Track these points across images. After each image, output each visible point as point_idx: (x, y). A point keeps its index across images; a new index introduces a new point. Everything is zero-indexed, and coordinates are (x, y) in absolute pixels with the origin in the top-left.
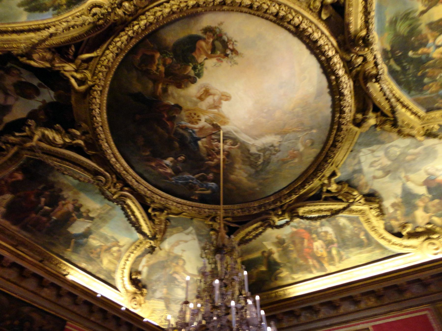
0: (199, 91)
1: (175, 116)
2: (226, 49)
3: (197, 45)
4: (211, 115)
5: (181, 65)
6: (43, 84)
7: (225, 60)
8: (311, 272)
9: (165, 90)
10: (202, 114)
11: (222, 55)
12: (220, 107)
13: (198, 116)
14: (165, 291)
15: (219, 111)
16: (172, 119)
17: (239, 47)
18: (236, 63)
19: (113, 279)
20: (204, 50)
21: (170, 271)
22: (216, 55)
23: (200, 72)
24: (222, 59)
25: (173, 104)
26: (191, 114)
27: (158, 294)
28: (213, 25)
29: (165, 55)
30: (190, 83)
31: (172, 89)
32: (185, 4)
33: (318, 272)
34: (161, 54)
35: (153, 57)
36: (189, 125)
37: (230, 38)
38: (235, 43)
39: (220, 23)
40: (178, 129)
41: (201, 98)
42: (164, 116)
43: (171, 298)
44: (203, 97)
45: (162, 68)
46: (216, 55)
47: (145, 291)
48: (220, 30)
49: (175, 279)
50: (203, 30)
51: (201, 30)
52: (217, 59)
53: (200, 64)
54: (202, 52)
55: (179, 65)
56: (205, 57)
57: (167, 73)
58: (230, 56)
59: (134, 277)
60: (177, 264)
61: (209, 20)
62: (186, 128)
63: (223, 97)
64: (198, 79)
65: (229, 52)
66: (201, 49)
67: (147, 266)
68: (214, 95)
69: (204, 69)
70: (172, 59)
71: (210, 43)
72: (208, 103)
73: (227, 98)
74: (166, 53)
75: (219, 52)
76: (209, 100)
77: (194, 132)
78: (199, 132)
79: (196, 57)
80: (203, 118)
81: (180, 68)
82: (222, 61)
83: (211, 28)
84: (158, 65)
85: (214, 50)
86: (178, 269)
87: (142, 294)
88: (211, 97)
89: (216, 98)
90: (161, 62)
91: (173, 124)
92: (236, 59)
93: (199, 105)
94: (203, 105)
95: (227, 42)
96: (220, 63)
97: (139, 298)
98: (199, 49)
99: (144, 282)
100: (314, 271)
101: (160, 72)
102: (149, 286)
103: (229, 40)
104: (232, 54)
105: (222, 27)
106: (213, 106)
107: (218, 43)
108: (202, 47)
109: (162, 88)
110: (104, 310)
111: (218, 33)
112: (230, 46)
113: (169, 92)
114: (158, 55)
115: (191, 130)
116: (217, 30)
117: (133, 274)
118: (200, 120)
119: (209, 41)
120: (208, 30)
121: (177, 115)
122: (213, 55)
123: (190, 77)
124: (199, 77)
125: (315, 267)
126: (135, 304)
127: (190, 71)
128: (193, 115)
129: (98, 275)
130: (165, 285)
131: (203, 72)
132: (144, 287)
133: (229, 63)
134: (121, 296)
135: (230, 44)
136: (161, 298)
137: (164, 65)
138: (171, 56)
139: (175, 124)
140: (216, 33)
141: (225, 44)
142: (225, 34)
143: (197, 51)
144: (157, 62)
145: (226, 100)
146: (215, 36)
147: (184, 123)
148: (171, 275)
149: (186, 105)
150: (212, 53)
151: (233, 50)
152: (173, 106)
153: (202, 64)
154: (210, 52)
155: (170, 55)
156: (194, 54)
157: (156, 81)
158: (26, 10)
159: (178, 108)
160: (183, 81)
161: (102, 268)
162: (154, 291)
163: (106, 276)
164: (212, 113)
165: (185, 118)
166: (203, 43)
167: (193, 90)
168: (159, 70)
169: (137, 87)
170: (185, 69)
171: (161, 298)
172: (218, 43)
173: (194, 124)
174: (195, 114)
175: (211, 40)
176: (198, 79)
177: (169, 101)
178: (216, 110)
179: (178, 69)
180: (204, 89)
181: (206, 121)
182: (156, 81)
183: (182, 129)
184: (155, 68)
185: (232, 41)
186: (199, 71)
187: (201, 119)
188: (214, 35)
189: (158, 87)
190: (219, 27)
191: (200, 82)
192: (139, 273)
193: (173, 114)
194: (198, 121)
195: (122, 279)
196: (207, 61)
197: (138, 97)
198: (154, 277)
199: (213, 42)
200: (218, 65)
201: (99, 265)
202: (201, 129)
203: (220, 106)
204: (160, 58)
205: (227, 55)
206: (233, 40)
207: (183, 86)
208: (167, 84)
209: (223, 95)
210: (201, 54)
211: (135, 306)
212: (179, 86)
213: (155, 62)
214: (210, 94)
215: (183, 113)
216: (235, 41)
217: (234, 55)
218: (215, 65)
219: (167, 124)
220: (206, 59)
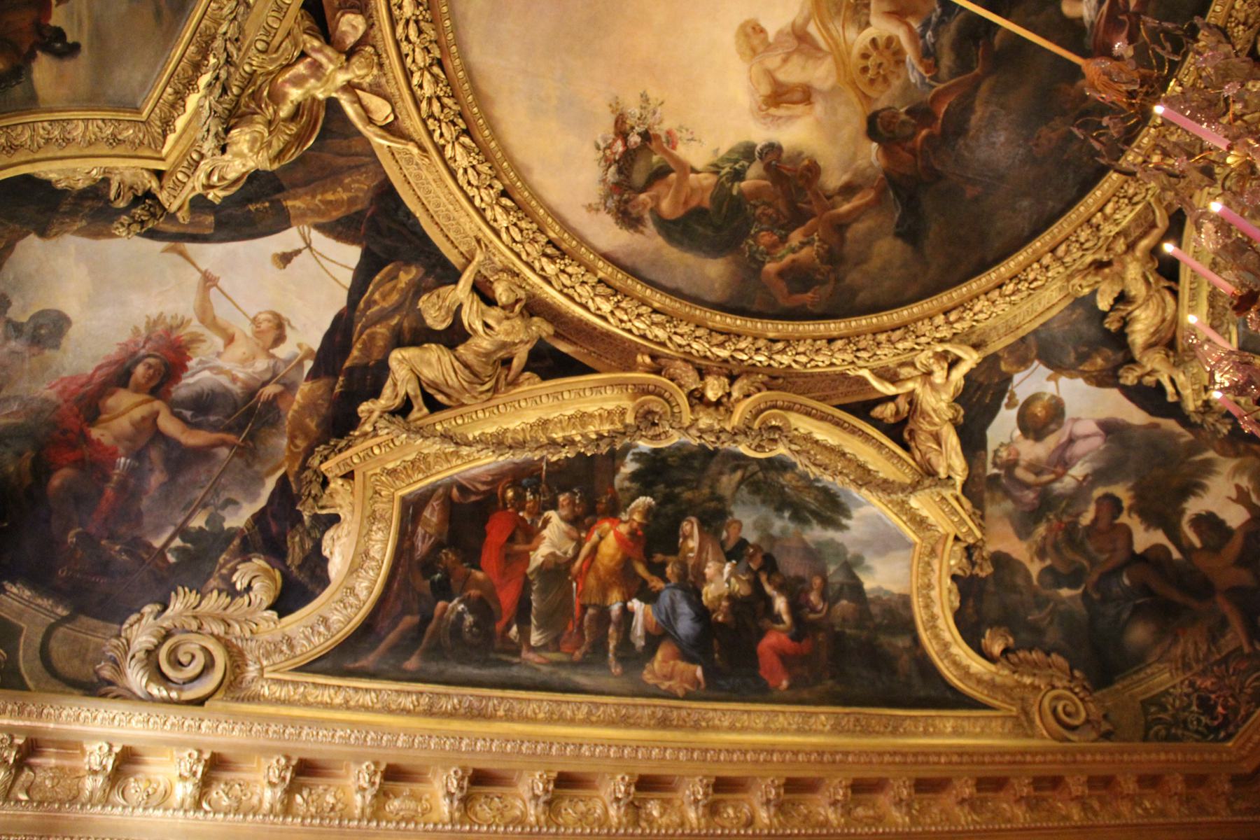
0: (790, 118)
1: (908, 112)
2: (634, 150)
3: (681, 212)
4: (836, 27)
5: (755, 207)
6: (1005, 400)
7: (660, 130)
9: (848, 190)
10: (849, 54)
11: (653, 146)
12: (793, 24)
13: (865, 56)
15: (807, 21)
16: (921, 113)
17: (605, 128)
18: (645, 98)
20: (678, 192)
22: (666, 158)
23: (736, 156)
24: (664, 139)
25: (875, 145)
26: (872, 81)
28: (609, 219)
29: (758, 257)
30: (784, 155)
31: (833, 179)
32: (617, 313)
34: (763, 263)
35: (781, 274)
36: (910, 56)
37: (603, 163)
38: (602, 145)
39: (593, 212)
40: (944, 71)
41: (806, 95)
42: (927, 138)
44: (797, 96)
45: (796, 237)
46: (666, 158)
48: (606, 198)
50: (637, 230)
51: (642, 232)
52: (674, 148)
53: (717, 173)
54: (686, 190)
55: (758, 211)
56: (692, 176)
57: (798, 217)
58: (637, 129)
61: (607, 234)
62: (928, 55)
63: (761, 49)
64: (758, 148)
65: (634, 139)
66: (682, 199)
68: (769, 73)
69: (723, 151)
70: (755, 237)
71: (652, 193)
72: (803, 68)
73: (752, 32)
74: (752, 258)
75: (655, 158)
76: (793, 73)
77: (926, 26)
78: (914, 13)
79: (708, 195)
80: (858, 40)
81: (764, 203)
82: (669, 133)
83: (617, 219)
84: (793, 251)
85: (660, 174)
88: (782, 76)
89: (773, 61)
90: (782, 251)
91: (937, 97)
92: (633, 110)
93: (827, 85)
94: (821, 74)
95: (616, 162)
96: (679, 134)
98: (686, 203)
101: (807, 234)
103: (608, 162)
104: (633, 128)
105: (595, 199)
106: (804, 46)
107: (639, 177)
108: (675, 203)
109: (848, 201)
111: (616, 197)
112: (619, 147)
113: (845, 178)
114: (771, 267)
115: (923, 37)
116: (611, 203)
118: (874, 41)
119: (649, 200)
120: (628, 218)
121: (902, 110)
122: (672, 166)
123: (768, 167)
124: (754, 146)
127: (754, 176)
128: (871, 74)
131: (731, 151)
133: (657, 115)
135: (615, 154)
137: (784, 240)
138: (751, 242)
139: (934, 90)
140: (619, 201)
141: (625, 163)
142: (604, 181)
143: (693, 203)
144: (790, 257)
145: (759, 30)
146: (626, 196)
147: (914, 70)
149: (852, 118)
150: (672, 171)
151: (622, 132)
152: (880, 143)
153: (715, 168)
154: (673, 176)
155: (750, 246)
156: (707, 203)
157: (840, 226)
158: (849, 517)
159: (875, 127)
160: (791, 178)
164: (828, 30)
165: (896, 83)
166: (665, 206)
167: (797, 133)
168: (805, 240)
169: (888, 248)
170: (757, 193)
172: (639, 177)
173: (899, 42)
174: (865, 70)
175: (643, 196)
176: (758, 148)
177: (873, 158)
178: (813, 29)
179: (769, 205)
180: (773, 111)
181: (868, 24)
182: (840, 226)
183: (936, 65)
184: (805, 253)
185: (606, 158)
186: (736, 162)
187: (868, 40)
188: (626, 202)
189: (850, 212)
190: (602, 208)
191: (760, 135)
193: (903, 123)
194: (881, 42)
196: (699, 165)
197: (910, 233)
199: (644, 189)
200: (685, 135)
202: (898, 14)
203: (789, 29)
204: (773, 260)
205: (646, 136)
206: (601, 153)
207: (806, 162)
208: (829, 198)
209: (754, 51)
210: (693, 190)
212: (813, 170)
213: (793, 261)
214: (776, 84)
215: (883, 100)
216: (598, 148)
217: (630, 122)
218: (692, 139)
219: (947, 112)
220: (694, 171)
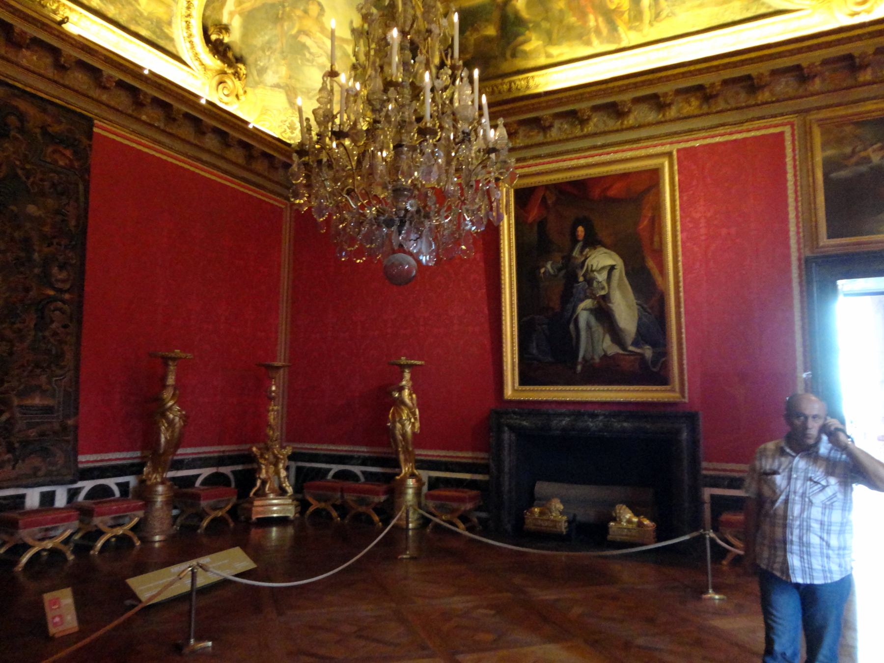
8: (588, 43)
14: (284, 70)
19: (171, 40)
21: (293, 28)
27: (270, 78)
33: (602, 43)
43: (298, 85)
47: (242, 69)
49: (304, 46)
59: (214, 37)
60: (306, 12)
67: (241, 14)
86: (308, 24)
87: (236, 74)
97: (231, 82)
99: (237, 50)
100: (595, 41)
102: (250, 60)
110: (163, 101)
117: (211, 30)
125: (598, 32)
126: (227, 96)
129: (133, 28)
130: (284, 58)
132: (240, 59)
134: (197, 76)
136: (277, 86)
148: (295, 37)
161: (141, 14)
162: (262, 71)
163: (154, 33)
171: (277, 86)
192: (225, 29)
195: (187, 37)
198: (259, 40)
201: (132, 5)
211: (226, 99)
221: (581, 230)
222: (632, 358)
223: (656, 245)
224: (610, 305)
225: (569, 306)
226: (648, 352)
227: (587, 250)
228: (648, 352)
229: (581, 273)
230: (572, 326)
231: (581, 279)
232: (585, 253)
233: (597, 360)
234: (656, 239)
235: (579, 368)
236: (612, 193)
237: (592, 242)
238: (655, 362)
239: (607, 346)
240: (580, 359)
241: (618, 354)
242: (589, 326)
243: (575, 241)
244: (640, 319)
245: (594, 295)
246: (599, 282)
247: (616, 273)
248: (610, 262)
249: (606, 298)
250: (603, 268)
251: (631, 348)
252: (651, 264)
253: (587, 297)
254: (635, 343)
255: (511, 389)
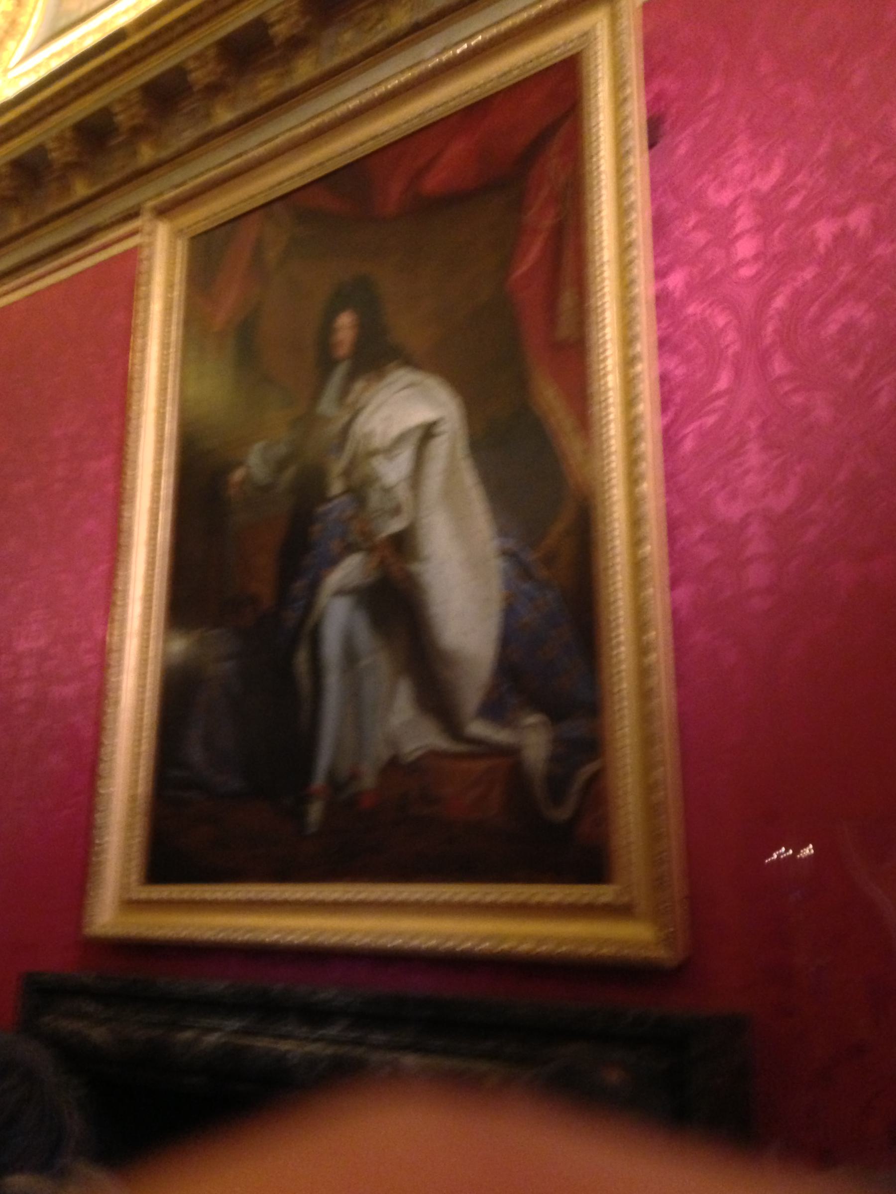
221: (345, 322)
222: (481, 765)
223: (564, 331)
224: (415, 567)
225: (299, 585)
226: (533, 740)
227: (359, 385)
228: (533, 740)
229: (337, 466)
230: (302, 658)
231: (336, 487)
232: (351, 398)
233: (369, 780)
234: (567, 300)
235: (315, 812)
236: (432, 183)
237: (376, 356)
238: (557, 784)
239: (404, 725)
240: (319, 780)
241: (435, 754)
242: (350, 656)
243: (326, 362)
244: (510, 612)
245: (367, 535)
246: (388, 491)
247: (440, 448)
248: (419, 414)
249: (404, 545)
250: (401, 439)
251: (478, 729)
252: (549, 396)
253: (350, 549)
254: (494, 709)
255: (116, 899)
